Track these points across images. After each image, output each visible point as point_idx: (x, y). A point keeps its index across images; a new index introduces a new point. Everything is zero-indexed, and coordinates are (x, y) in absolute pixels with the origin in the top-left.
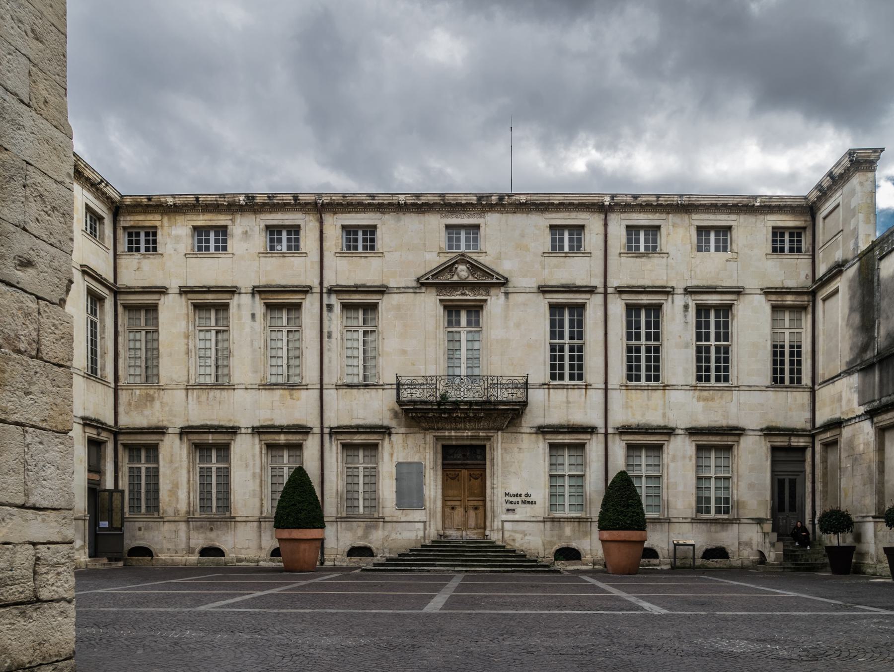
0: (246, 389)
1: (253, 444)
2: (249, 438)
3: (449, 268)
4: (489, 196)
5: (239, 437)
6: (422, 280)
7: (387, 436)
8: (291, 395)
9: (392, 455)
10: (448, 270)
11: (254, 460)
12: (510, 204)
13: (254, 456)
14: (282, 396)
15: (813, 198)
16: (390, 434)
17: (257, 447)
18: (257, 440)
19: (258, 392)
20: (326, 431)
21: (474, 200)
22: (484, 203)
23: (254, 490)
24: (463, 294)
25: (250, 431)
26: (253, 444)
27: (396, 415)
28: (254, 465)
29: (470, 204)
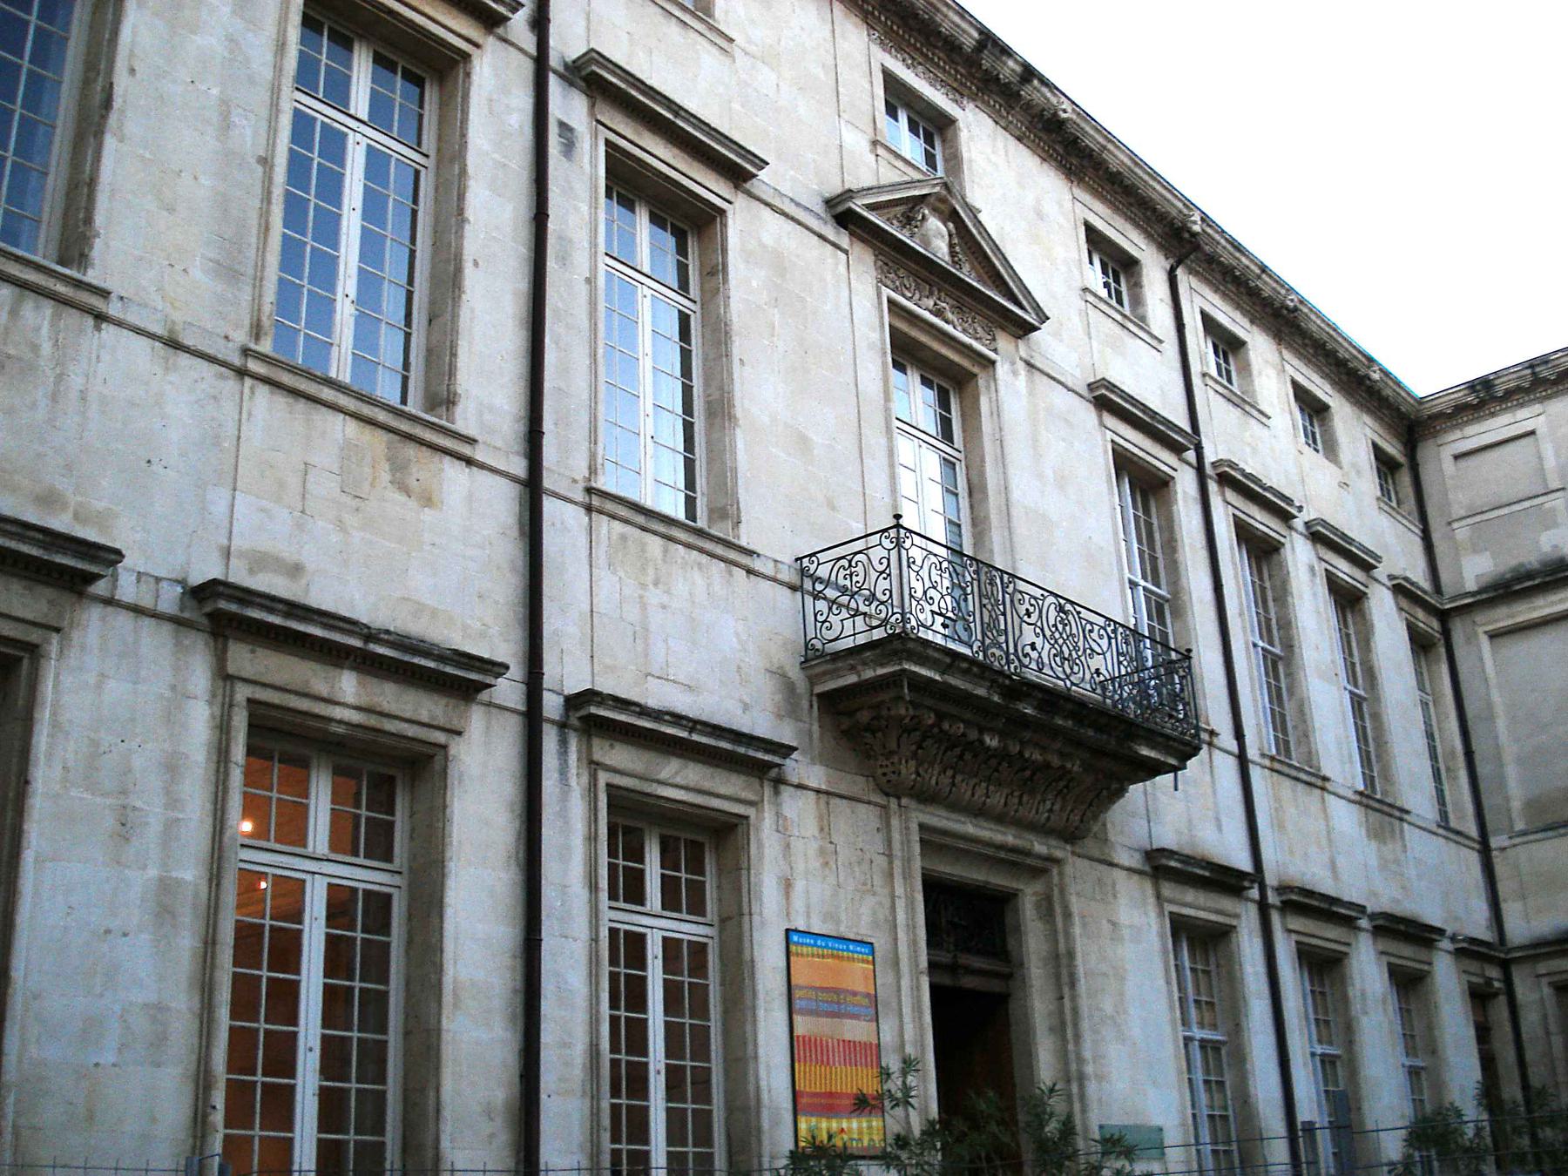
0: (174, 344)
1: (179, 695)
2: (154, 641)
3: (910, 210)
4: (1006, 51)
5: (94, 629)
6: (858, 205)
7: (768, 791)
8: (399, 468)
9: (787, 885)
10: (900, 209)
11: (173, 802)
12: (1028, 106)
13: (172, 767)
14: (348, 450)
15: (1443, 405)
16: (779, 782)
17: (199, 719)
18: (199, 676)
19: (231, 384)
20: (552, 705)
21: (970, 38)
22: (986, 64)
23: (157, 1010)
24: (939, 313)
25: (169, 599)
26: (179, 695)
27: (790, 705)
28: (171, 826)
29: (951, 46)
